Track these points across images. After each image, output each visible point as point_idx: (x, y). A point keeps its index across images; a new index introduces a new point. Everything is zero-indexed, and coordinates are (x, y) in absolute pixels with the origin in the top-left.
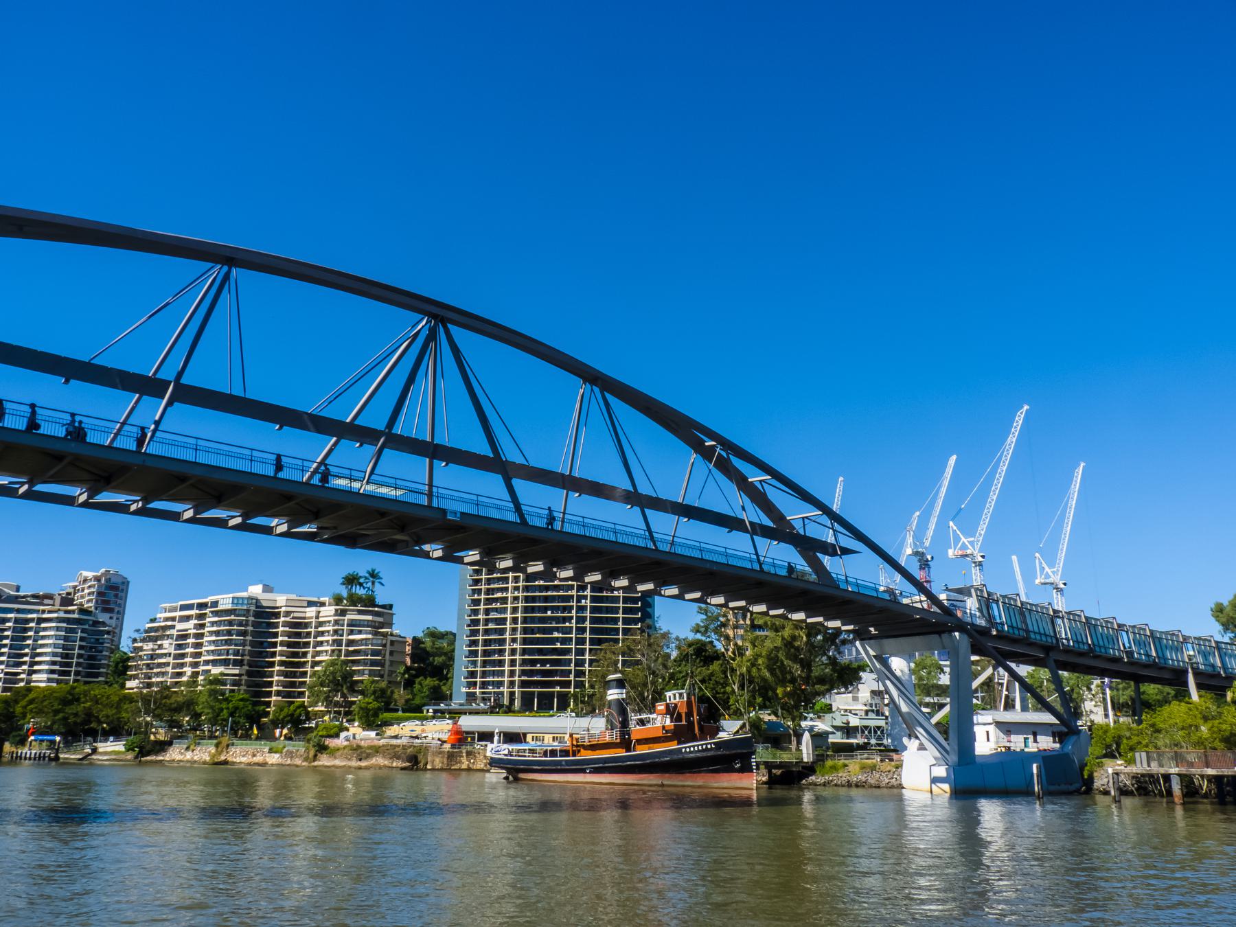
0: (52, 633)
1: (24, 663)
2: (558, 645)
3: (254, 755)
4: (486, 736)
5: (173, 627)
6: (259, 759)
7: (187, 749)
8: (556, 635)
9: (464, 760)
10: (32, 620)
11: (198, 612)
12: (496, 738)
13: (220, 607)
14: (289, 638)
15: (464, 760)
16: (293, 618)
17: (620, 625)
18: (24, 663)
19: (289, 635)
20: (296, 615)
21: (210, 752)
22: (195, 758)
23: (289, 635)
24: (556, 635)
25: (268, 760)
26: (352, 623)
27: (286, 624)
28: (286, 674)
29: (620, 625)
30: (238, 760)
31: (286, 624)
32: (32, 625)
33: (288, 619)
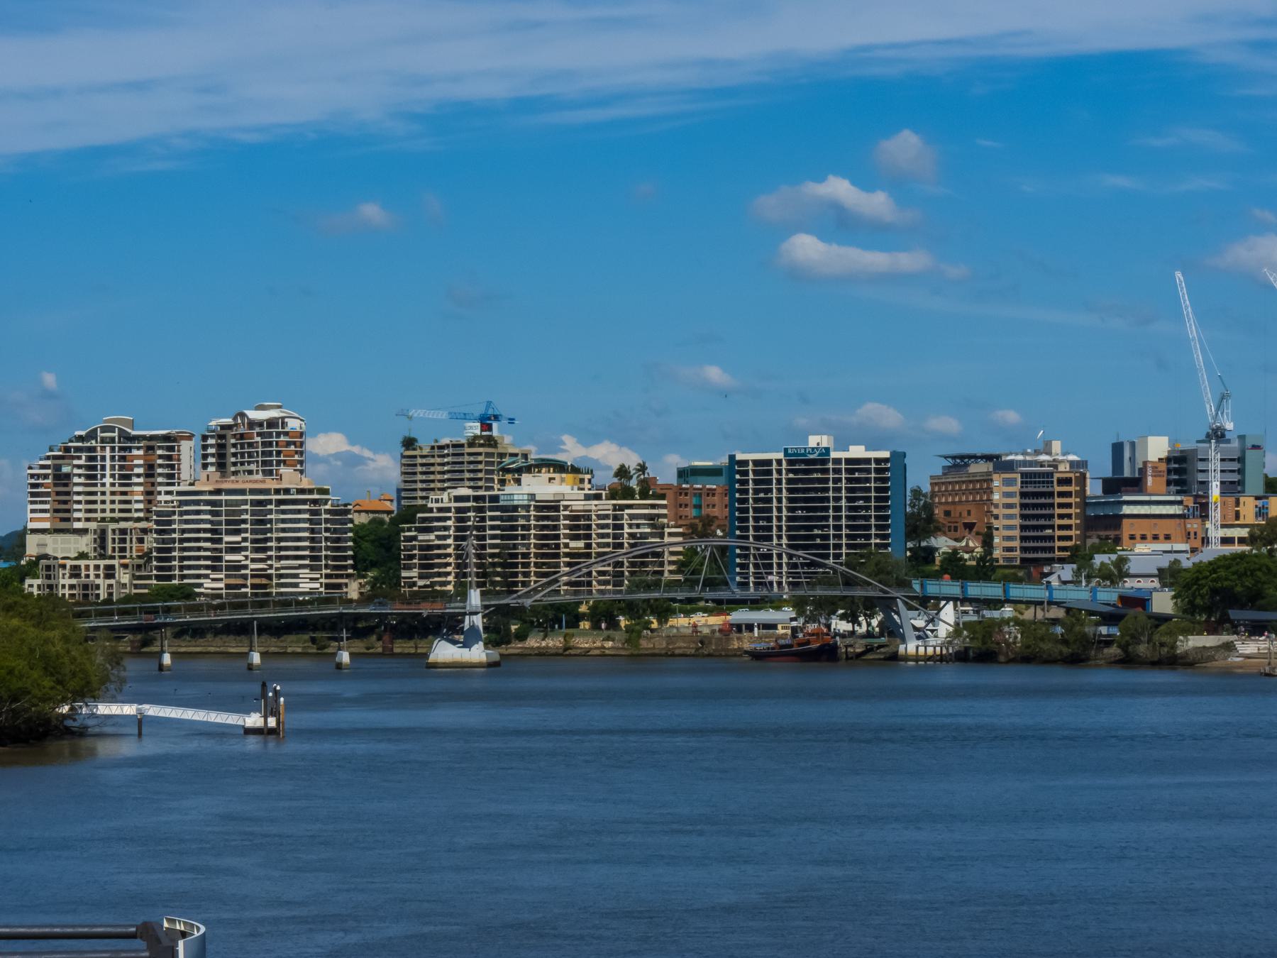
0: (307, 516)
1: (270, 549)
2: (818, 541)
3: (594, 643)
4: (750, 627)
5: (449, 518)
6: (598, 644)
7: (543, 639)
8: (816, 532)
9: (736, 643)
10: (270, 502)
11: (474, 504)
12: (756, 629)
13: (501, 503)
14: (571, 530)
15: (736, 643)
16: (571, 511)
17: (873, 522)
18: (270, 549)
19: (571, 528)
20: (574, 508)
21: (560, 641)
22: (550, 645)
23: (571, 528)
24: (816, 532)
25: (605, 645)
26: (632, 517)
27: (566, 517)
28: (569, 564)
29: (873, 522)
30: (582, 646)
31: (566, 517)
32: (272, 507)
33: (567, 513)
